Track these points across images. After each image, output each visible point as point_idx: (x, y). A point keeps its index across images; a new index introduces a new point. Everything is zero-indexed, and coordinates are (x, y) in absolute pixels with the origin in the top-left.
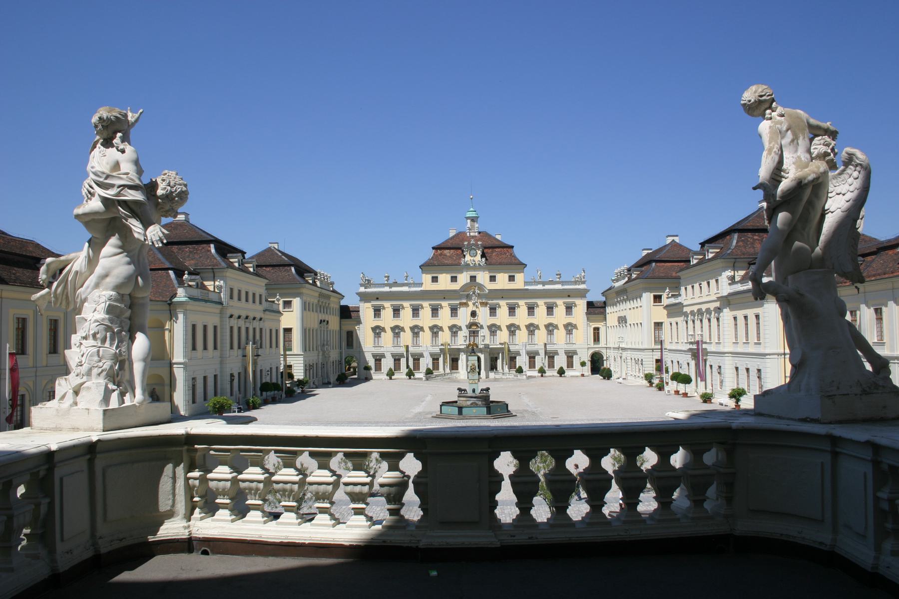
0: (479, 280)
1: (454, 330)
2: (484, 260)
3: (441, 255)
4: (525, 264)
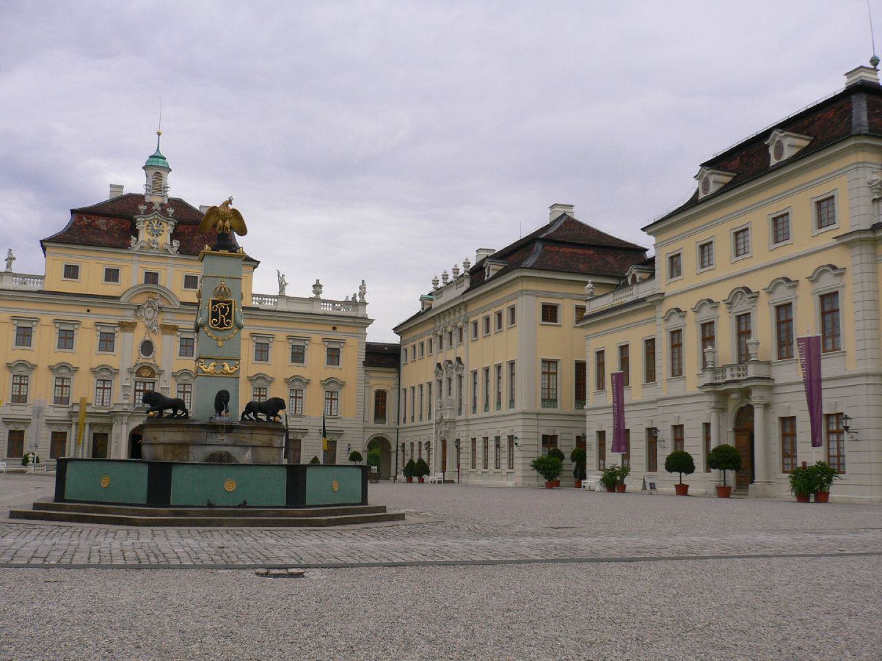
0: (161, 281)
1: (104, 376)
2: (176, 243)
3: (89, 226)
4: (255, 261)
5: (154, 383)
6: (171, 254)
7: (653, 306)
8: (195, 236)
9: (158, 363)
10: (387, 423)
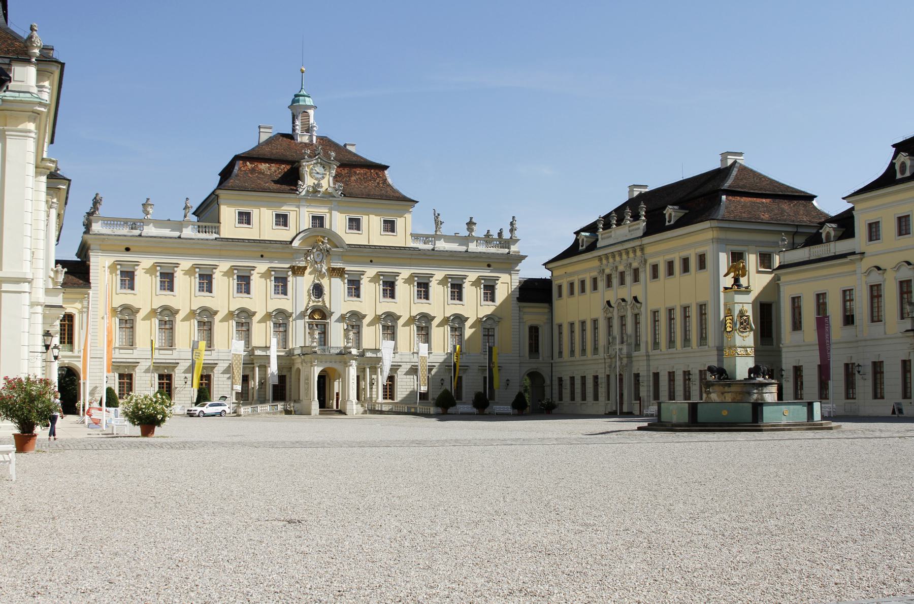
3: (253, 171)
5: (325, 325)
6: (335, 197)
7: (852, 262)
8: (351, 177)
9: (328, 305)
10: (541, 359)
